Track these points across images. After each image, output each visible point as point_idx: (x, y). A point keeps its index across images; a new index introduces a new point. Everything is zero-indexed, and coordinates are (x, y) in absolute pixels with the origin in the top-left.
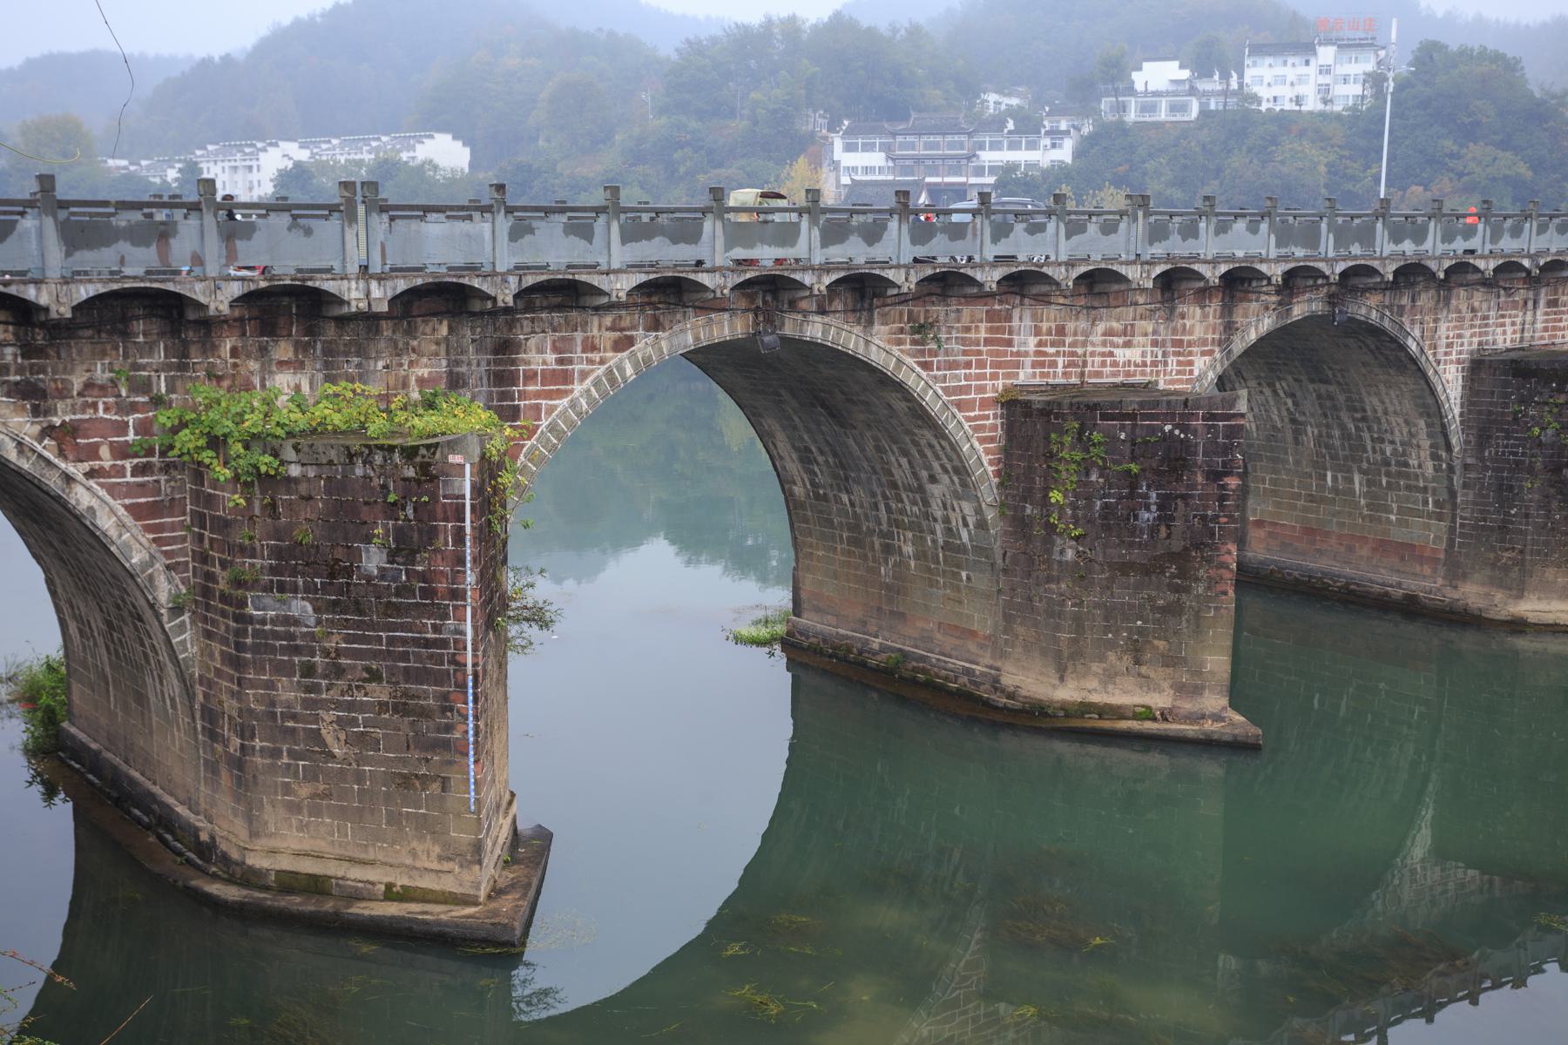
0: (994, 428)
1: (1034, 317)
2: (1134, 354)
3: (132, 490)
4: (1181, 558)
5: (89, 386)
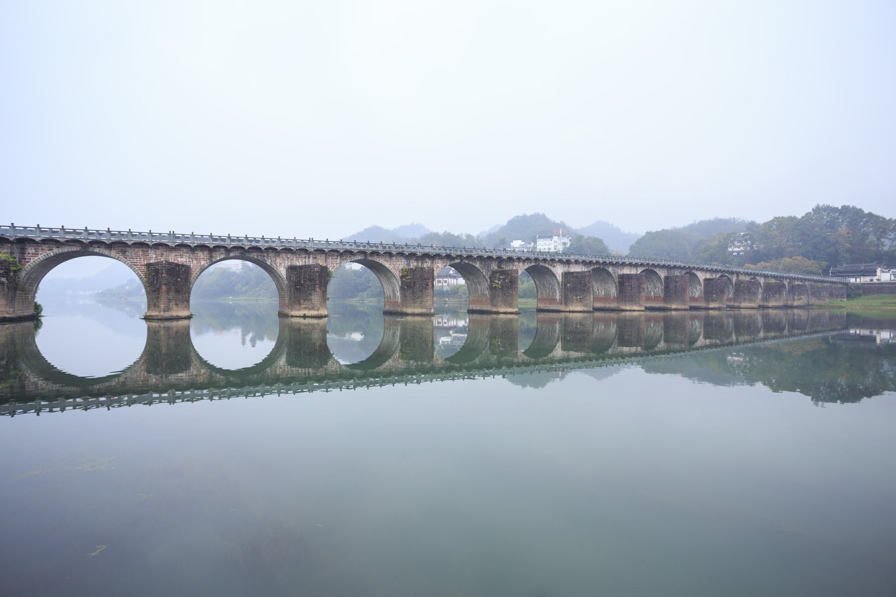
0: (144, 269)
1: (155, 251)
2: (184, 260)
4: (158, 289)
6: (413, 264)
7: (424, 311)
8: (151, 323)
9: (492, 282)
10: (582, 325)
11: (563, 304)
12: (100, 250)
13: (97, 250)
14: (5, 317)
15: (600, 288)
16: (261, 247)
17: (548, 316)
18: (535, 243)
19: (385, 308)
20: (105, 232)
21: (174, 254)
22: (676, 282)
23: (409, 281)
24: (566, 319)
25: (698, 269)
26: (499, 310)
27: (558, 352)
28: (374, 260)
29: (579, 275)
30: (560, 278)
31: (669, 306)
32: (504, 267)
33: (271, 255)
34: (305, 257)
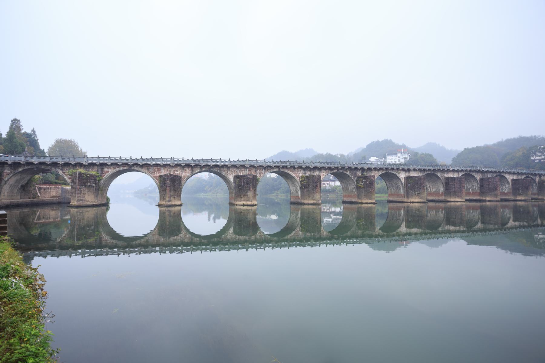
1: (164, 169)
2: (178, 173)
3: (69, 177)
5: (66, 170)
6: (308, 173)
7: (315, 202)
8: (162, 208)
9: (357, 183)
10: (419, 211)
11: (406, 198)
12: (137, 169)
13: (136, 168)
14: (94, 204)
15: (431, 187)
16: (219, 165)
17: (395, 205)
18: (385, 158)
19: (291, 200)
20: (140, 159)
21: (173, 170)
22: (489, 182)
23: (306, 183)
24: (408, 207)
25: (506, 173)
26: (362, 201)
27: (403, 229)
28: (284, 171)
29: (416, 178)
30: (403, 181)
31: (484, 199)
32: (366, 174)
33: (225, 169)
34: (244, 170)
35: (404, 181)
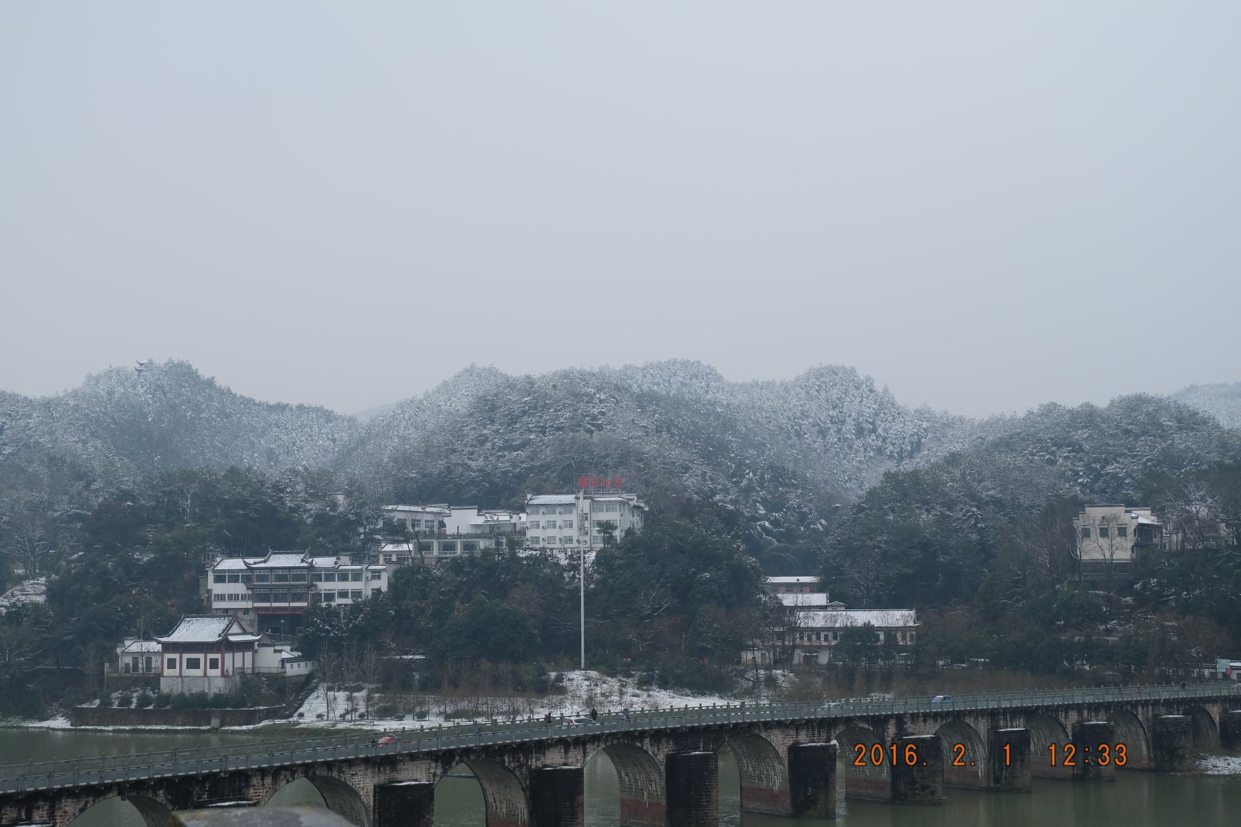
15: (497, 796)
35: (372, 798)
